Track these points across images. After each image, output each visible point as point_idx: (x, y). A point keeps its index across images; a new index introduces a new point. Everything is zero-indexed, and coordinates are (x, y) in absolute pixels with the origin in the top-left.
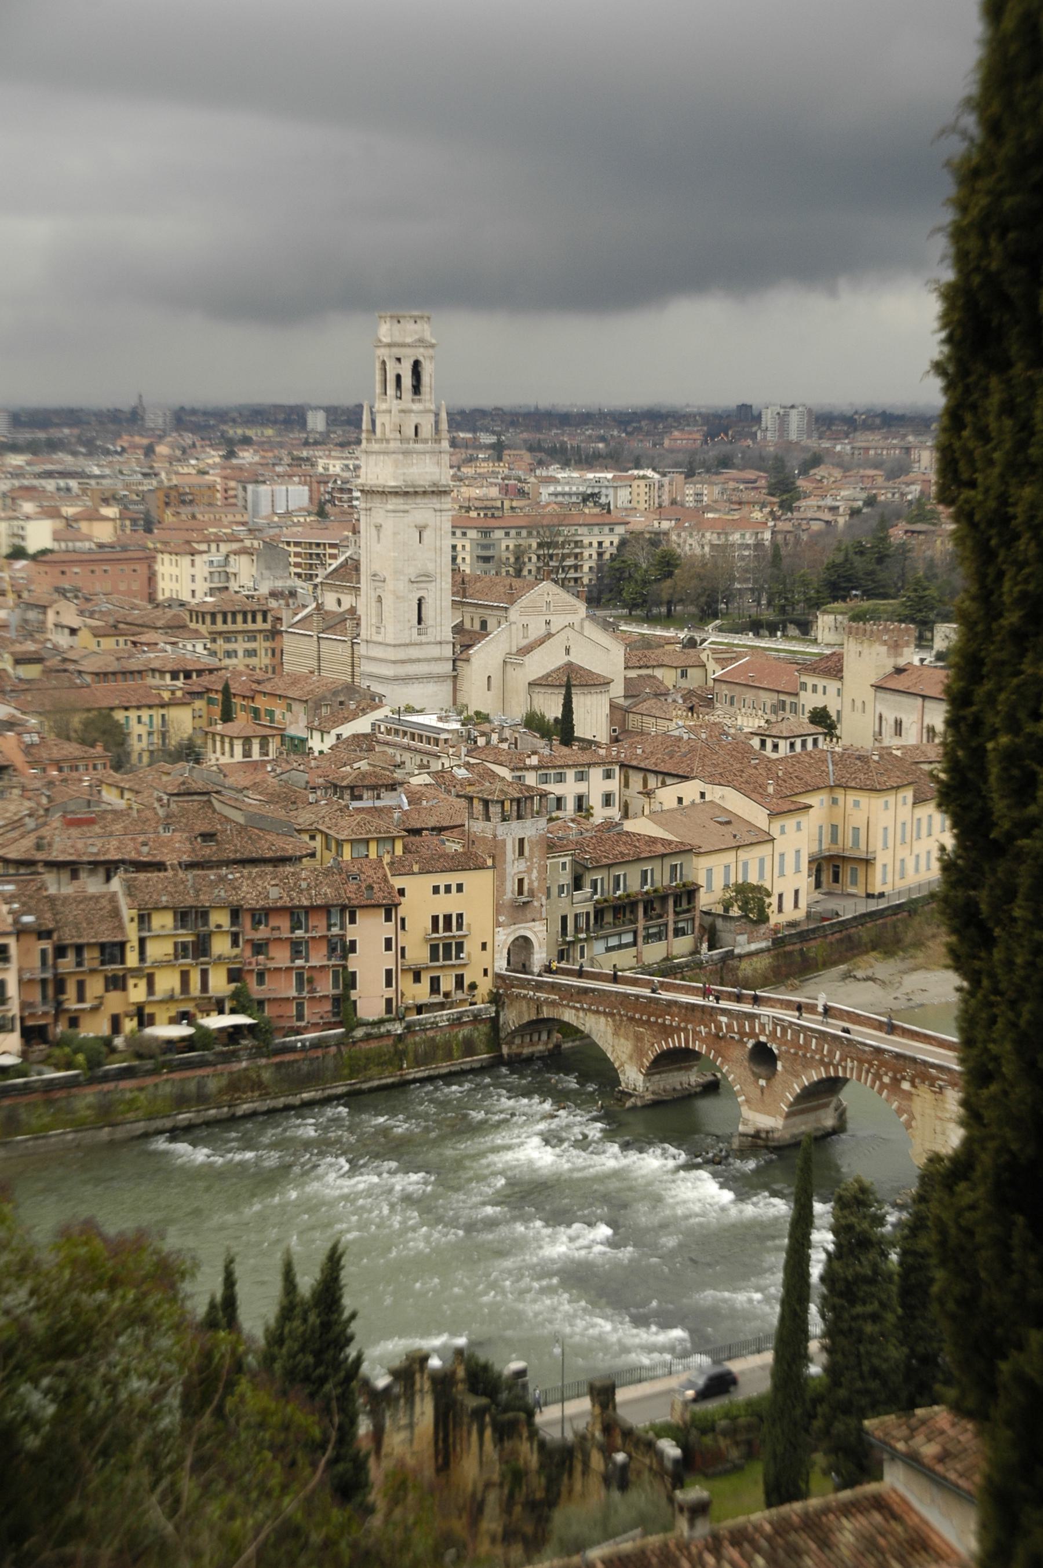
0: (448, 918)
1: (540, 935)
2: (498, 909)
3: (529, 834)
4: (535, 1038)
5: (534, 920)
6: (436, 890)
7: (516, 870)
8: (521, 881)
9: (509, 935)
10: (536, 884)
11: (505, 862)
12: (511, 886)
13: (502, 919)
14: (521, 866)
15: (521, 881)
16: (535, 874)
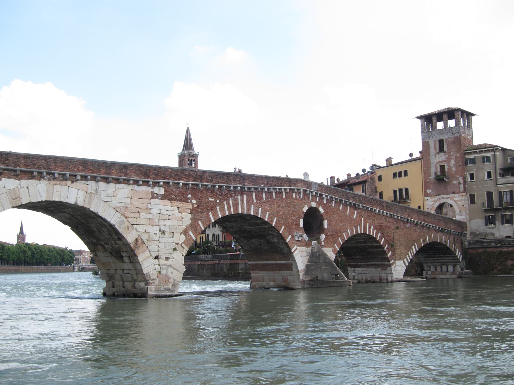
0: (401, 191)
1: (460, 203)
2: (426, 185)
3: (447, 137)
4: (444, 268)
5: (454, 193)
6: (395, 175)
7: (437, 160)
8: (442, 167)
9: (435, 202)
10: (454, 169)
11: (429, 155)
12: (435, 169)
13: (429, 191)
14: (442, 157)
15: (442, 167)
16: (452, 162)
